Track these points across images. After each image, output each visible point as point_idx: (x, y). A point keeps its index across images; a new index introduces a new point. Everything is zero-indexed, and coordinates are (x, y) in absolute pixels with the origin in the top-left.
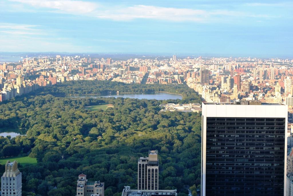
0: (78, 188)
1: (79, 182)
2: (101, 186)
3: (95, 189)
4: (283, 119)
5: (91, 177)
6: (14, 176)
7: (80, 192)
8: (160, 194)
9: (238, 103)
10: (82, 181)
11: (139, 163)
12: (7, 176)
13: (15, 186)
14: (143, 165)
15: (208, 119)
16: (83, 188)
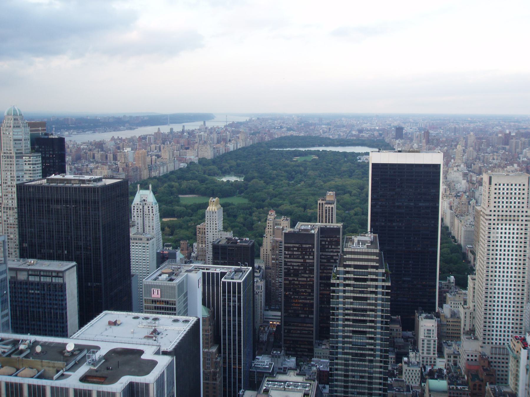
0: (268, 222)
1: (269, 217)
2: (287, 220)
3: (282, 222)
4: (440, 165)
5: (280, 214)
6: (216, 210)
7: (269, 225)
8: (328, 227)
9: (400, 151)
10: (272, 215)
11: (319, 202)
12: (211, 210)
13: (217, 218)
14: (322, 204)
15: (373, 164)
16: (272, 222)
